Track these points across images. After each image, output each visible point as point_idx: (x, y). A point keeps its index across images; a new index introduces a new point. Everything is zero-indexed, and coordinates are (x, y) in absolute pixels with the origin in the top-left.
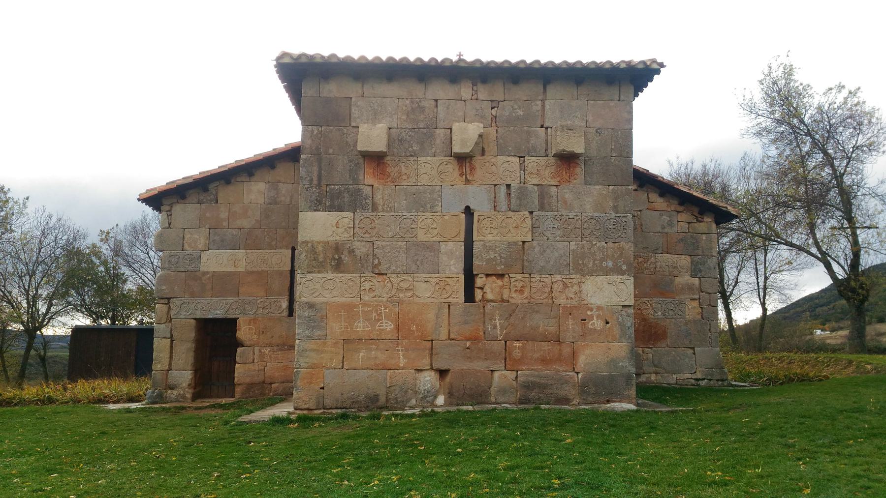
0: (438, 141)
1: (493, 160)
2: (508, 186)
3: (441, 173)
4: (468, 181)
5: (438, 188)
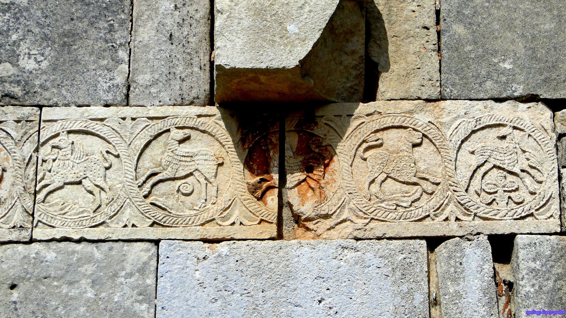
0: (145, 33)
1: (422, 119)
2: (502, 247)
3: (154, 180)
4: (289, 222)
5: (139, 253)
